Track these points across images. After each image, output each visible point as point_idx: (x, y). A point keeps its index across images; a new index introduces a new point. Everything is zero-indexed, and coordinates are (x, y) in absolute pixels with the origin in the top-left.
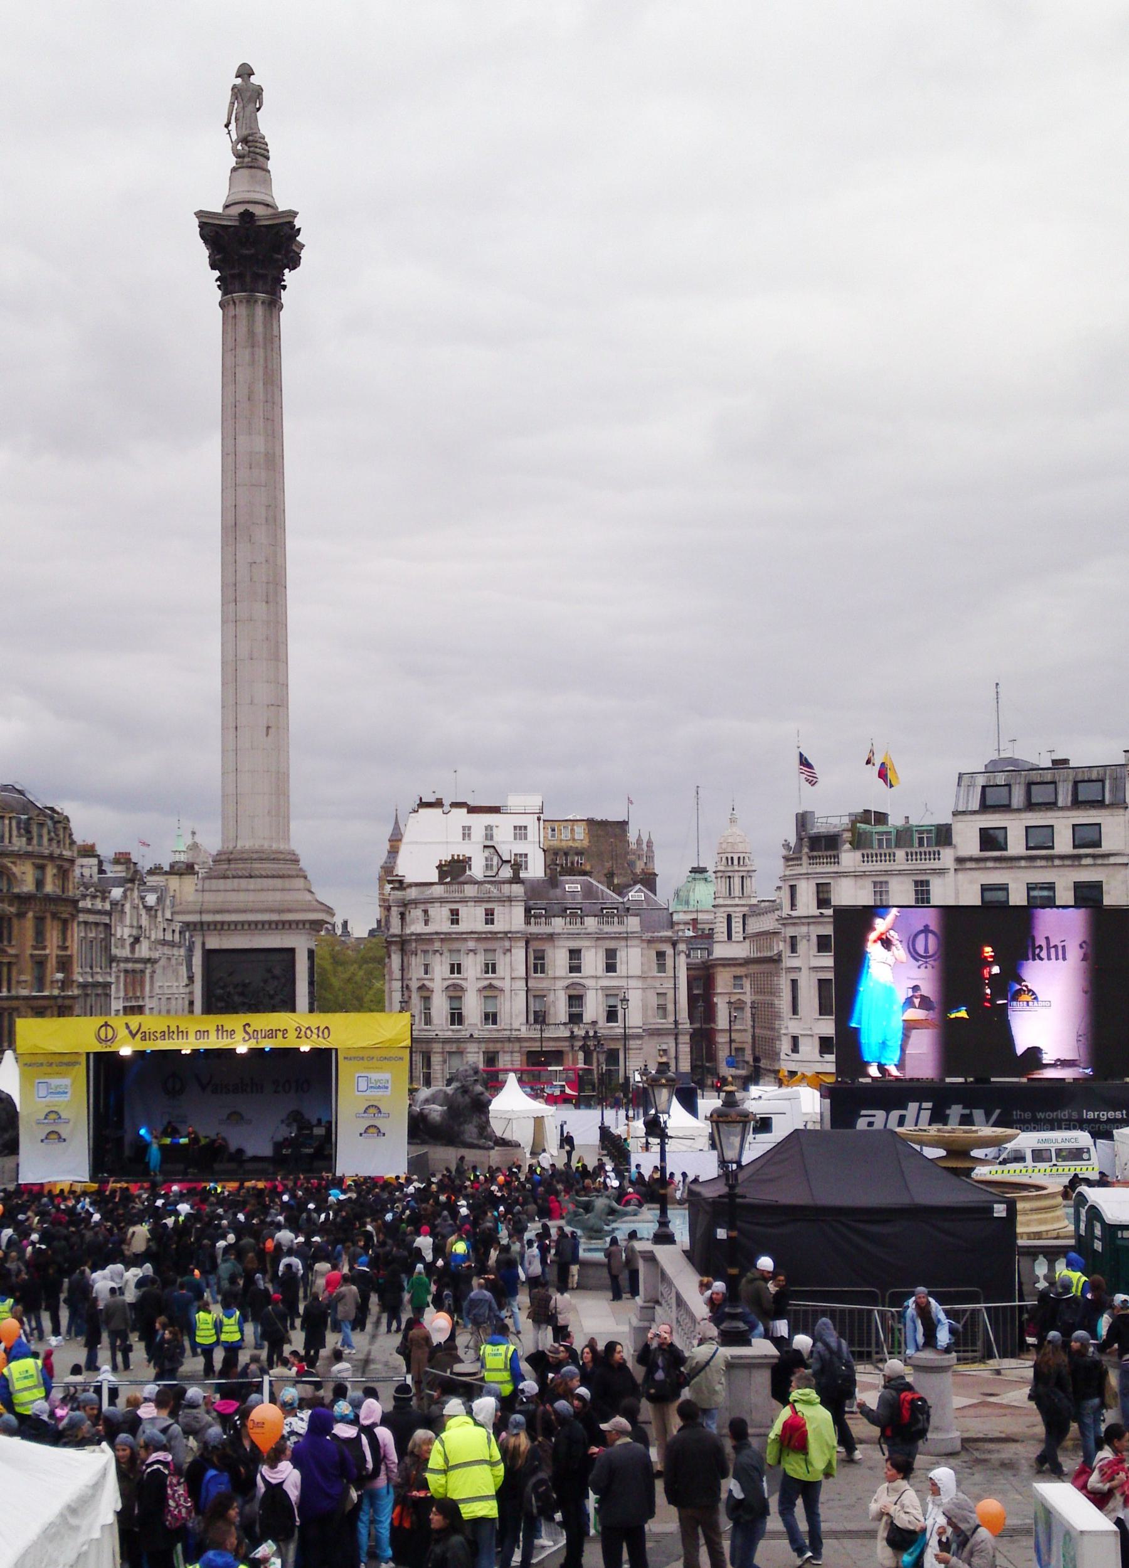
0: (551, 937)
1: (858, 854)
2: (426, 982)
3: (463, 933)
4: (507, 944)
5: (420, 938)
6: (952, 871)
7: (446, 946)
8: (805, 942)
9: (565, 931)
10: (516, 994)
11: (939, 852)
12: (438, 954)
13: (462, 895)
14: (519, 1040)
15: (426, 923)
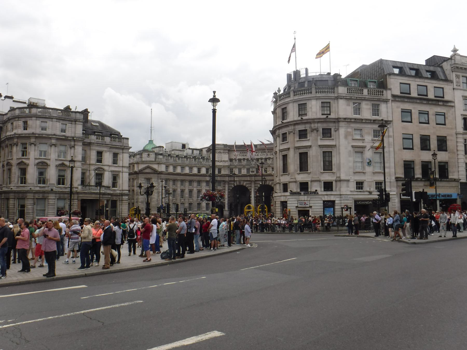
0: (90, 144)
1: (346, 88)
2: (24, 160)
3: (49, 135)
4: (72, 143)
5: (20, 137)
6: (391, 101)
7: (38, 141)
8: (315, 131)
9: (96, 142)
10: (76, 169)
11: (382, 93)
12: (33, 145)
13: (49, 115)
14: (78, 193)
15: (25, 128)
